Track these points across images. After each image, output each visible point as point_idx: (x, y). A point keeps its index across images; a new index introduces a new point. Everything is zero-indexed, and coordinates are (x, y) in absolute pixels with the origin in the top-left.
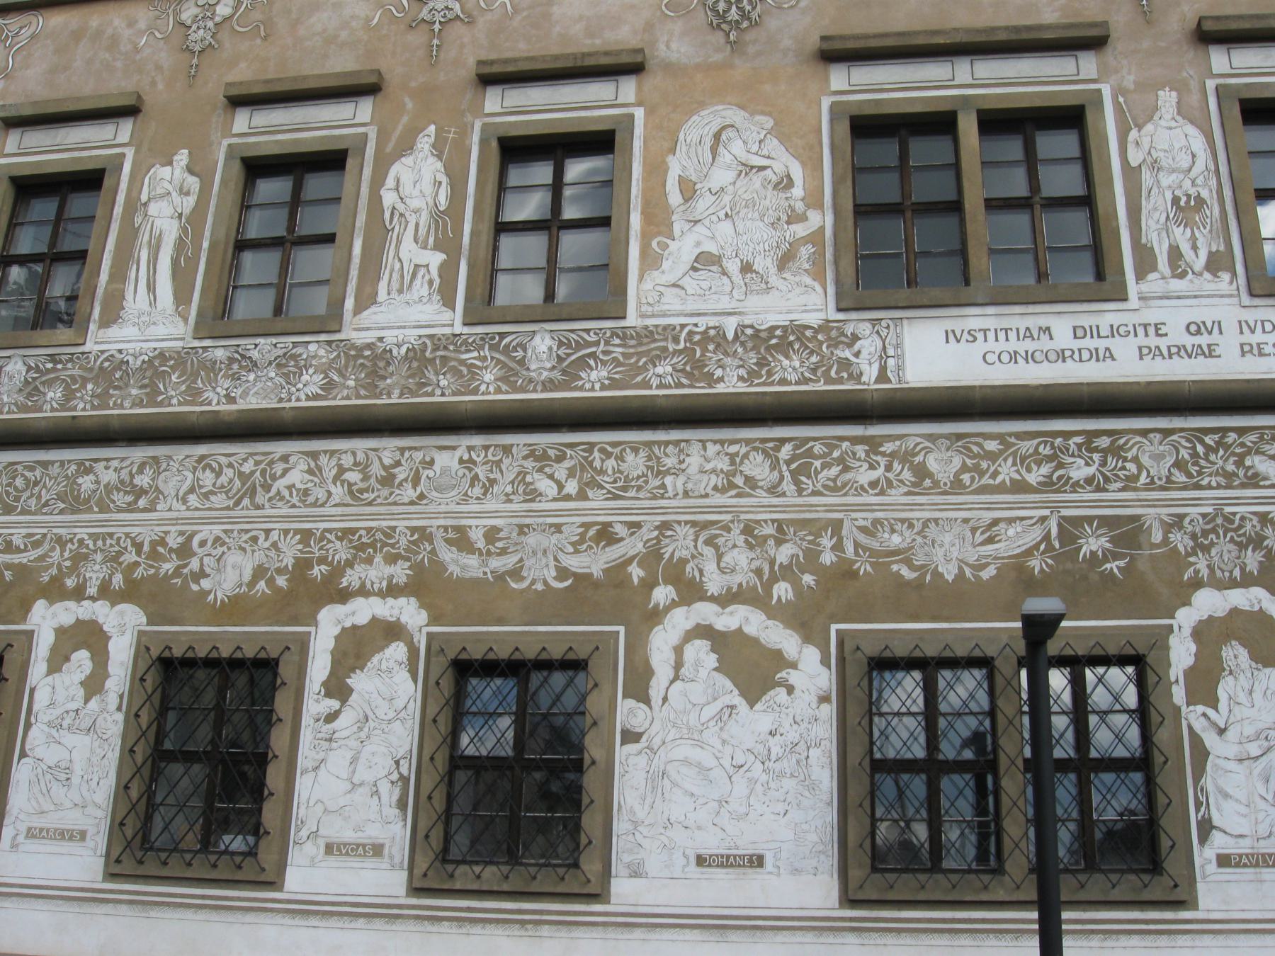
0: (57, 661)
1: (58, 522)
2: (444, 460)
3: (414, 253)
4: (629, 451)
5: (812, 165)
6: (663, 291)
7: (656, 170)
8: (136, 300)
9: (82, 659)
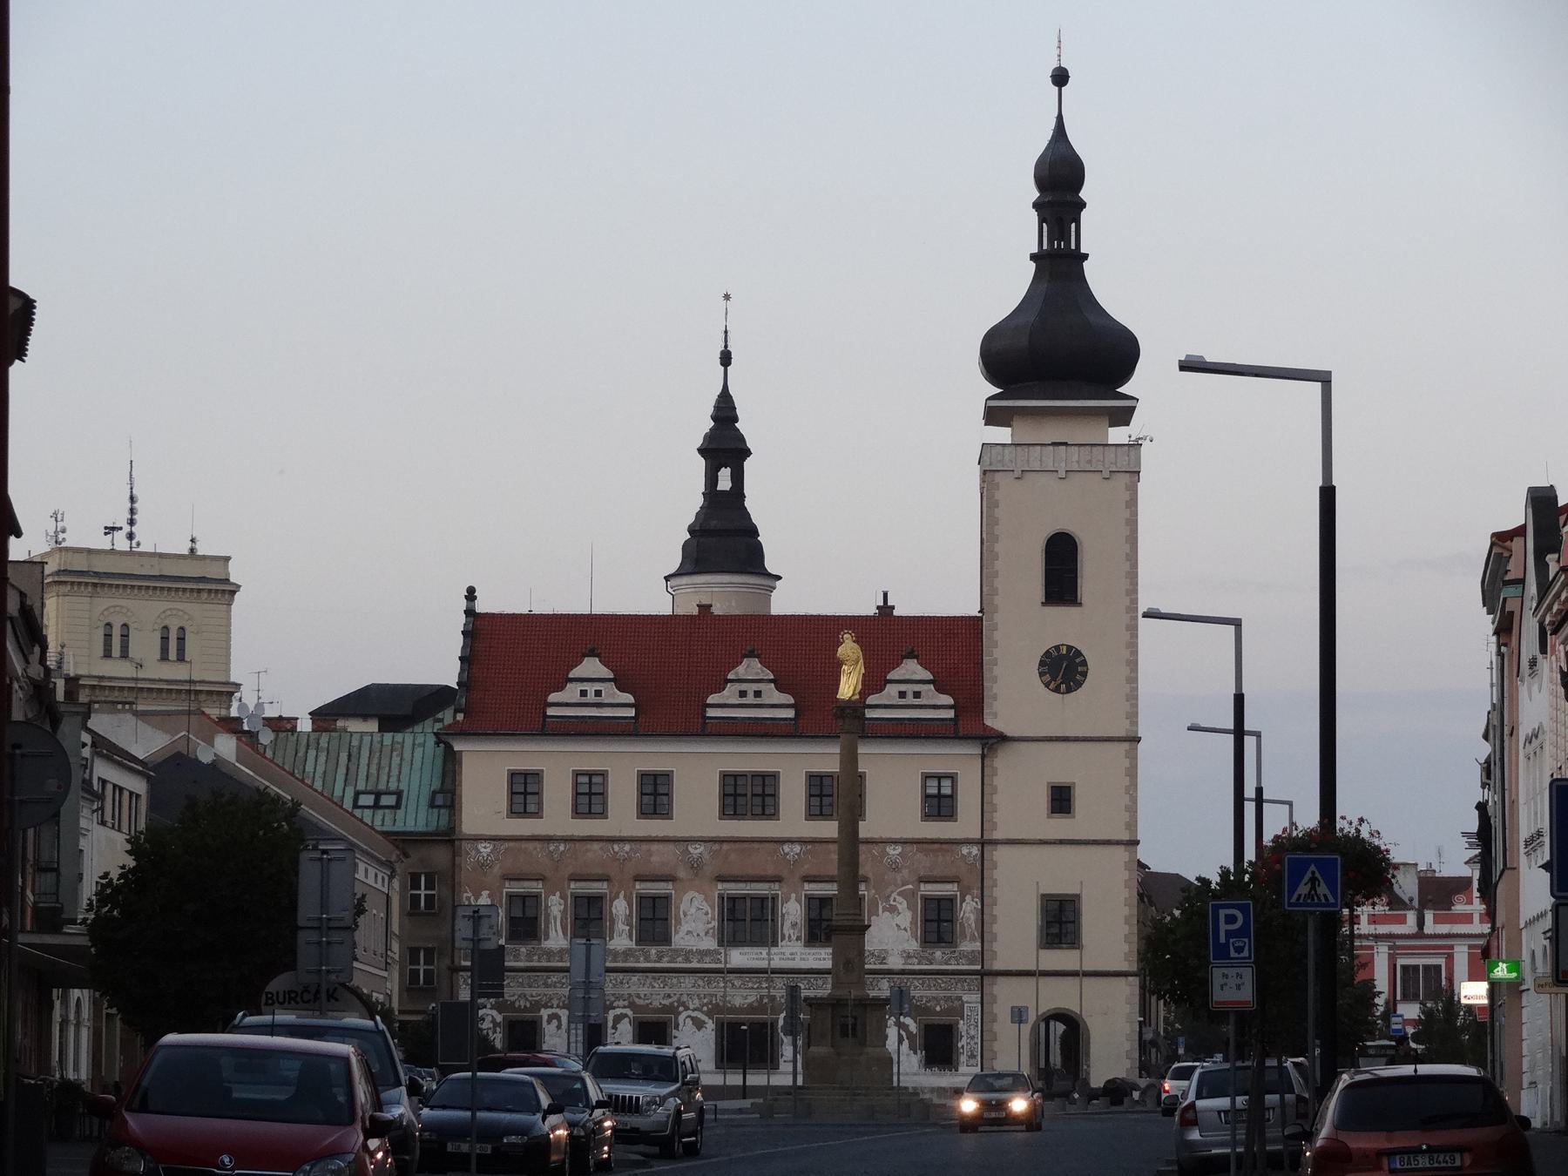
0: (549, 1022)
1: (542, 990)
2: (635, 979)
3: (621, 926)
4: (674, 979)
5: (713, 908)
6: (680, 939)
7: (678, 908)
8: (552, 934)
9: (555, 1022)
